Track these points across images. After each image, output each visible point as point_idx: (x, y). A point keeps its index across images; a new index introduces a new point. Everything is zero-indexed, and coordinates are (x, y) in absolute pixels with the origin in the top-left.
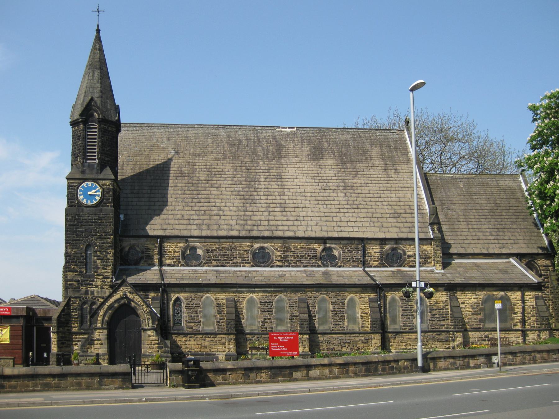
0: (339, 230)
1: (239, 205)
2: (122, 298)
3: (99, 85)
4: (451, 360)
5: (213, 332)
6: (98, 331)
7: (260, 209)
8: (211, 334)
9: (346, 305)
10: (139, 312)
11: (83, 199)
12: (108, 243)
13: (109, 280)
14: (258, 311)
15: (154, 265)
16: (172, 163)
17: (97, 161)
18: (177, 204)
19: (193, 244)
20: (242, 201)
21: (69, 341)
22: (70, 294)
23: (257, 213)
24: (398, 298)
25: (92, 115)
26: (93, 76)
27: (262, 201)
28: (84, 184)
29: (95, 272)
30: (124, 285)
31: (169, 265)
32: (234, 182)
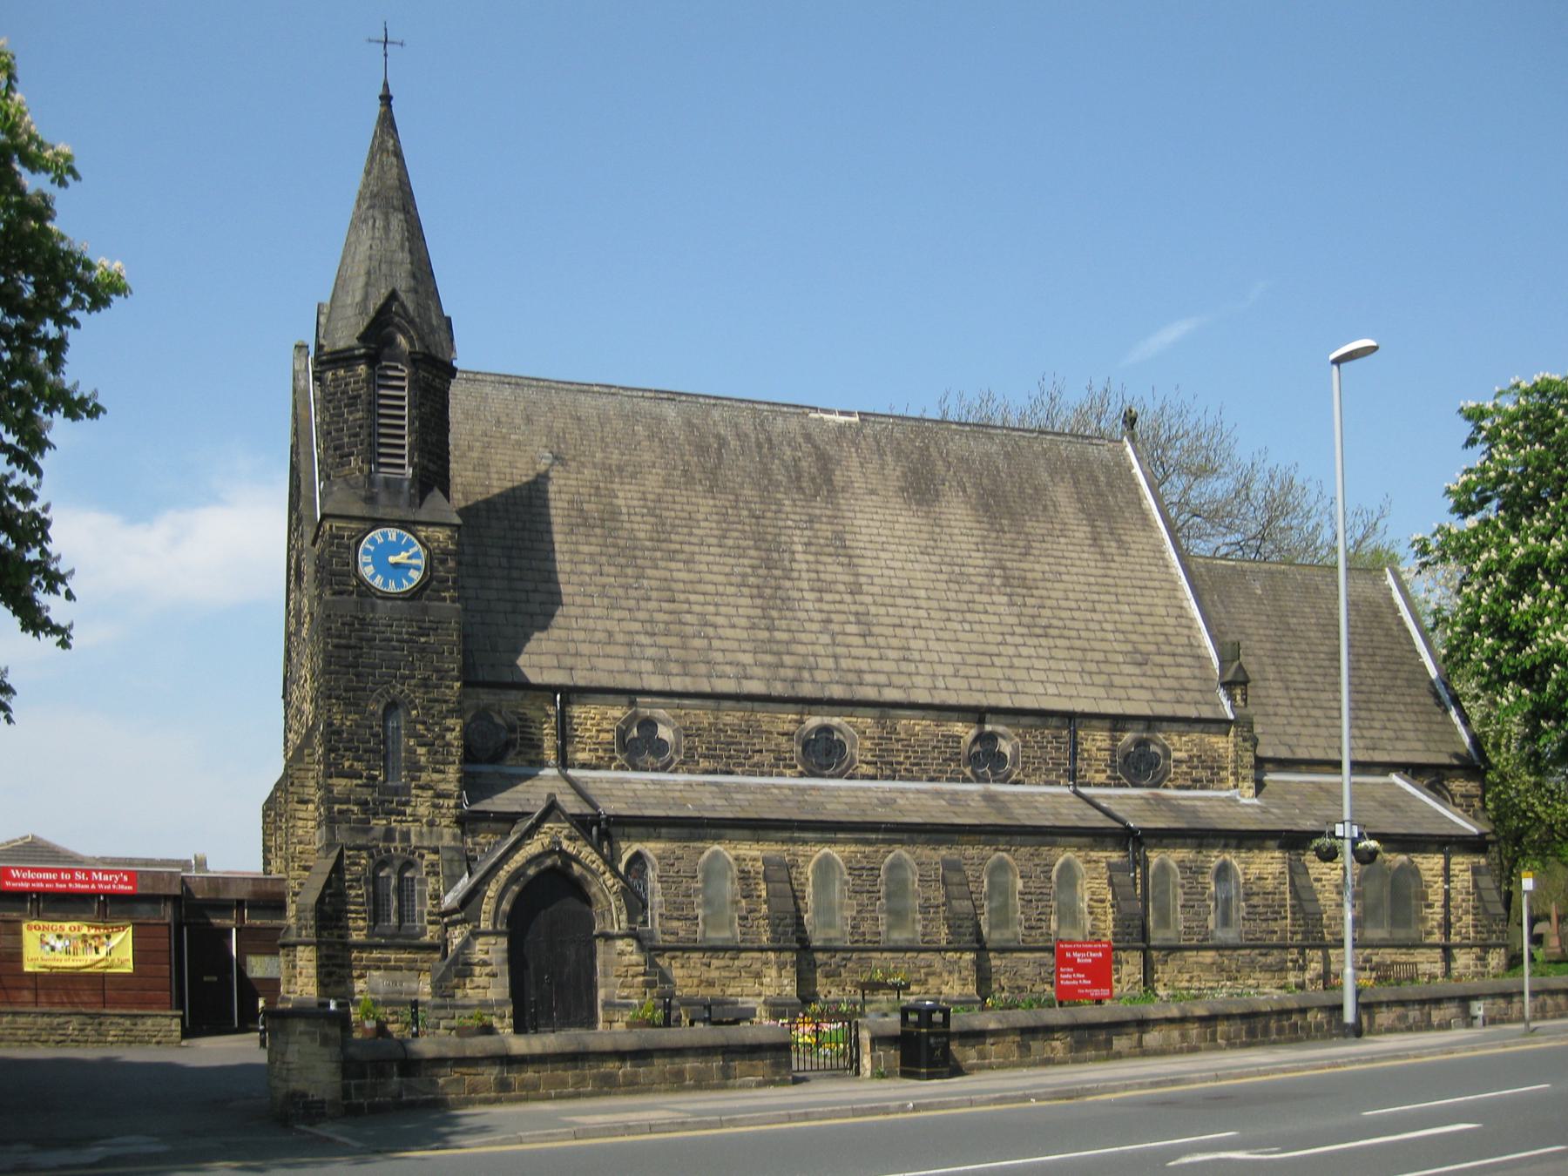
0: (1012, 688)
1: (752, 612)
2: (548, 853)
3: (406, 255)
4: (1398, 1010)
5: (731, 944)
6: (482, 940)
7: (807, 625)
8: (726, 949)
9: (1054, 878)
10: (594, 889)
11: (373, 577)
12: (446, 702)
13: (452, 803)
14: (842, 891)
15: (543, 764)
16: (552, 488)
17: (409, 471)
18: (588, 601)
19: (648, 712)
20: (759, 602)
21: (342, 966)
22: (342, 837)
23: (803, 637)
24: (1174, 865)
25: (391, 341)
26: (387, 228)
27: (809, 605)
28: (377, 534)
29: (413, 779)
30: (552, 817)
31: (584, 766)
32: (726, 551)
